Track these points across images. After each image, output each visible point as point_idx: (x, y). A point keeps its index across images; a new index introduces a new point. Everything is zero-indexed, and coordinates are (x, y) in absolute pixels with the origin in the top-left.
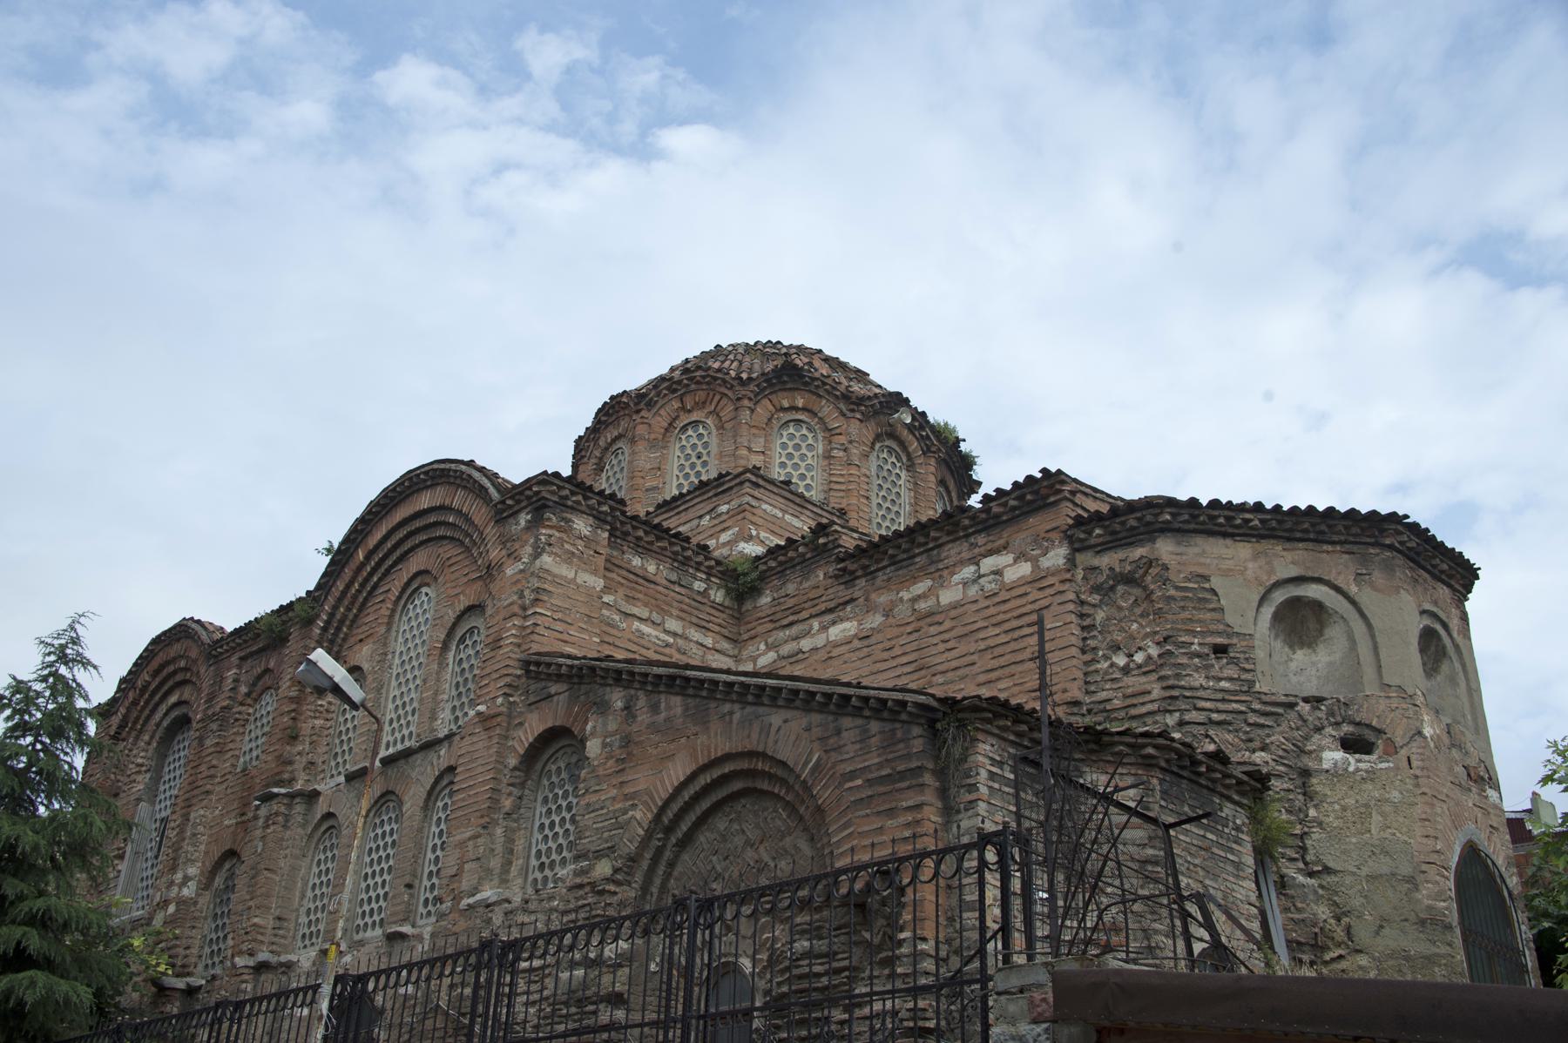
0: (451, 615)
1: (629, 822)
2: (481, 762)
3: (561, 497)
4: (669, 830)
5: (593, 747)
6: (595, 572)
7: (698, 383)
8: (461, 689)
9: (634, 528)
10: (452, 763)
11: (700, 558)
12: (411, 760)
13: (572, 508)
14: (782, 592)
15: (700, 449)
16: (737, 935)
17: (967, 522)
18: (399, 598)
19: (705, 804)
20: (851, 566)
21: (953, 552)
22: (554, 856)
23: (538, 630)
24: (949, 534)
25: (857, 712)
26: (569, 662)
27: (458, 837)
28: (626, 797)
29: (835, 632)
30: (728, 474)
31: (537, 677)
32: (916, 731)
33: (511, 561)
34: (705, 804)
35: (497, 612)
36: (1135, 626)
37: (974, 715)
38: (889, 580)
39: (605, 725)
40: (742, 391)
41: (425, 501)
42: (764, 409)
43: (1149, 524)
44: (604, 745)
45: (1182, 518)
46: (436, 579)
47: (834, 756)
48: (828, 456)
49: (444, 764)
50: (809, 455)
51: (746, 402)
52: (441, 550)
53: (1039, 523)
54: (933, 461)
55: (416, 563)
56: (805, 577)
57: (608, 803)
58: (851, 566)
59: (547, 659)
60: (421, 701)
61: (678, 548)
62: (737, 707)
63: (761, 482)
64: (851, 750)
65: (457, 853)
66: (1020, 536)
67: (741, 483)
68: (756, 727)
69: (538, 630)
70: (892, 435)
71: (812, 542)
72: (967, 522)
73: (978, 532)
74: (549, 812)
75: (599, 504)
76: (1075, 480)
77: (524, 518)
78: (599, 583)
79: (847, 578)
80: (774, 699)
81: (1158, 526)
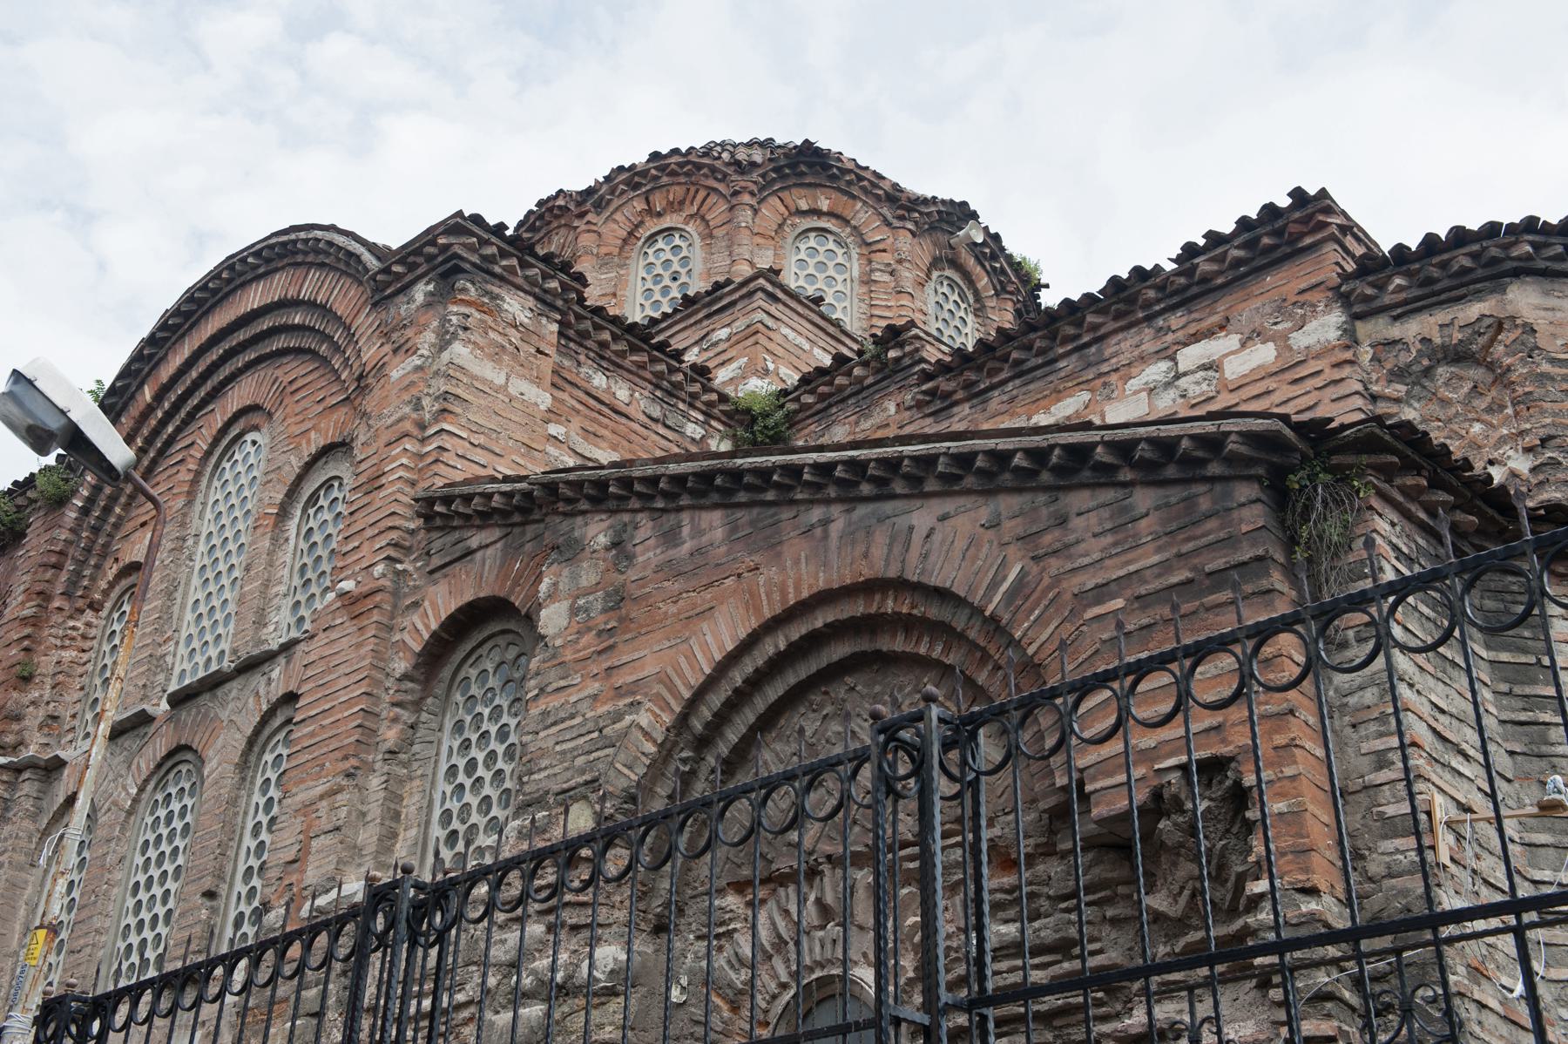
0: (296, 463)
1: (625, 733)
2: (345, 672)
3: (484, 258)
4: (703, 743)
5: (552, 619)
6: (537, 381)
7: (673, 174)
8: (309, 574)
9: (597, 327)
10: (292, 687)
11: (696, 388)
12: (219, 692)
13: (501, 278)
15: (676, 267)
16: (843, 925)
17: (1151, 294)
18: (208, 454)
19: (774, 691)
20: (944, 384)
21: (1123, 346)
22: (475, 818)
23: (445, 457)
24: (1116, 318)
25: (1105, 476)
26: (506, 487)
27: (298, 798)
28: (619, 692)
30: (728, 282)
31: (446, 529)
32: (1245, 491)
33: (398, 359)
34: (774, 691)
35: (376, 436)
36: (1477, 428)
37: (1365, 459)
38: (1012, 400)
39: (575, 577)
40: (739, 181)
41: (254, 298)
42: (772, 210)
43: (1495, 261)
44: (574, 611)
45: (1550, 252)
46: (270, 415)
47: (1055, 565)
48: (867, 281)
49: (277, 691)
50: (840, 278)
51: (746, 198)
52: (279, 372)
53: (1284, 281)
54: (1009, 306)
55: (235, 399)
56: (864, 413)
57: (583, 707)
58: (944, 384)
59: (466, 490)
60: (241, 601)
61: (662, 367)
62: (836, 510)
63: (780, 295)
64: (1093, 549)
65: (298, 824)
66: (1252, 305)
67: (751, 294)
68: (881, 538)
69: (445, 457)
70: (955, 264)
71: (877, 357)
72: (1151, 294)
73: (1172, 309)
74: (466, 745)
75: (545, 277)
76: (1344, 213)
77: (420, 292)
78: (544, 399)
79: (938, 405)
80: (915, 481)
81: (1509, 265)
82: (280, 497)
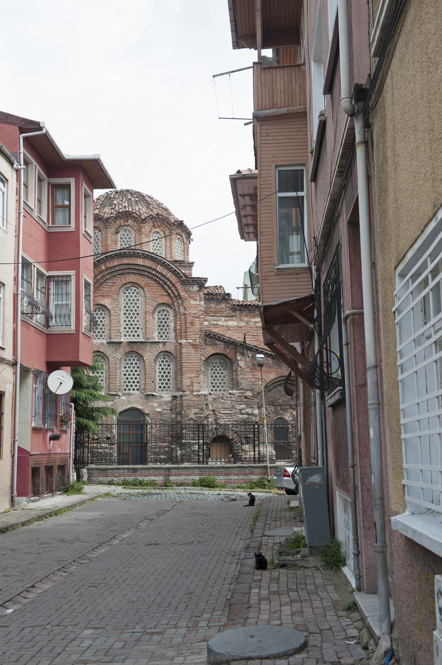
14: (210, 306)
19: (277, 384)
28: (255, 378)
29: (230, 323)
82: (153, 309)
